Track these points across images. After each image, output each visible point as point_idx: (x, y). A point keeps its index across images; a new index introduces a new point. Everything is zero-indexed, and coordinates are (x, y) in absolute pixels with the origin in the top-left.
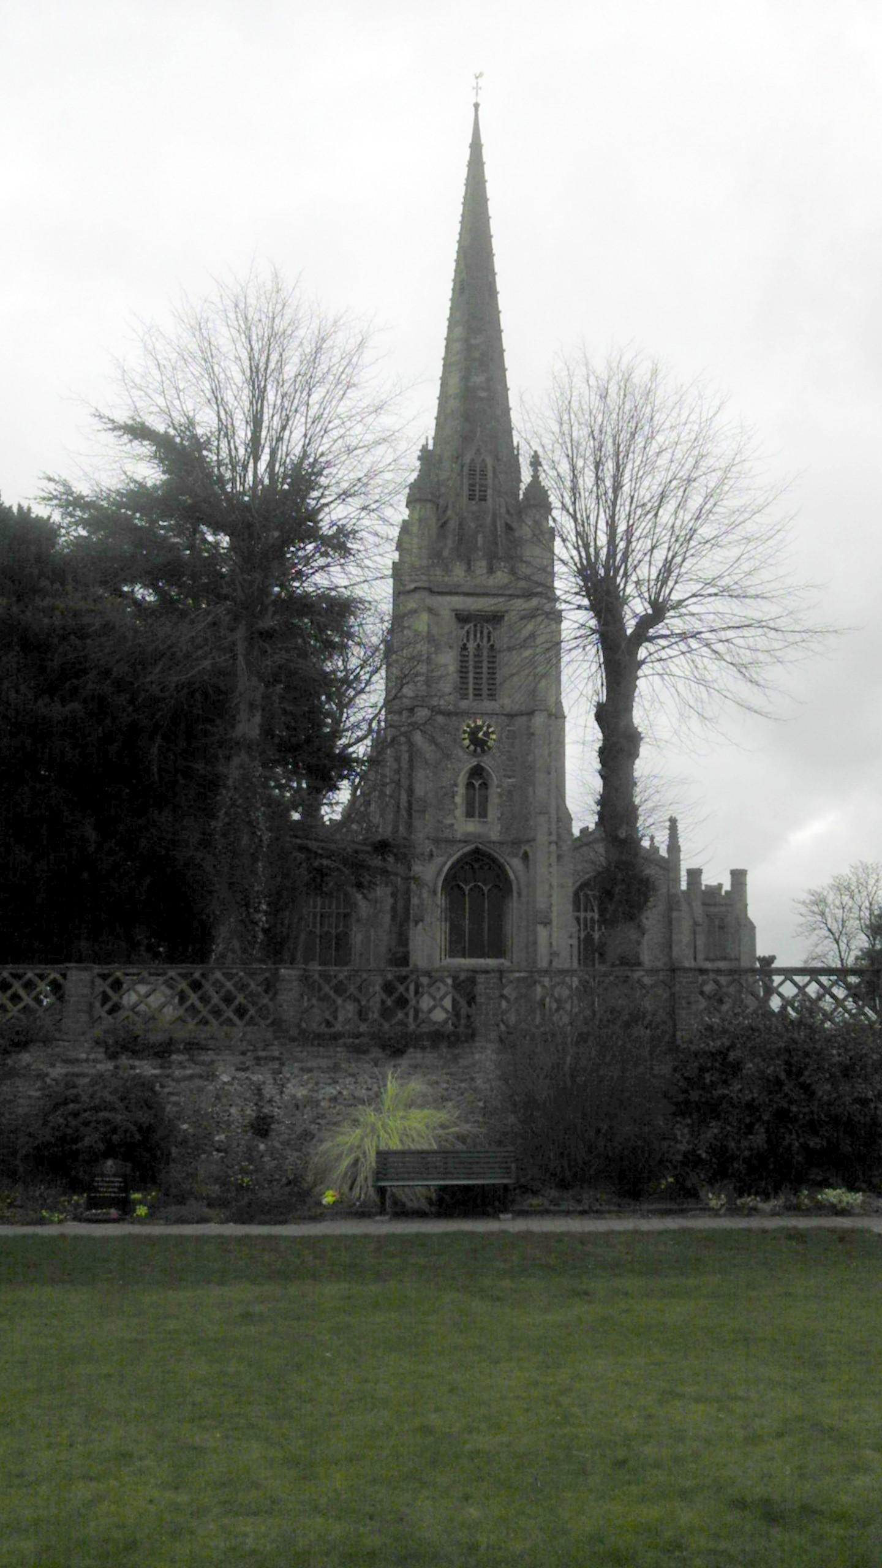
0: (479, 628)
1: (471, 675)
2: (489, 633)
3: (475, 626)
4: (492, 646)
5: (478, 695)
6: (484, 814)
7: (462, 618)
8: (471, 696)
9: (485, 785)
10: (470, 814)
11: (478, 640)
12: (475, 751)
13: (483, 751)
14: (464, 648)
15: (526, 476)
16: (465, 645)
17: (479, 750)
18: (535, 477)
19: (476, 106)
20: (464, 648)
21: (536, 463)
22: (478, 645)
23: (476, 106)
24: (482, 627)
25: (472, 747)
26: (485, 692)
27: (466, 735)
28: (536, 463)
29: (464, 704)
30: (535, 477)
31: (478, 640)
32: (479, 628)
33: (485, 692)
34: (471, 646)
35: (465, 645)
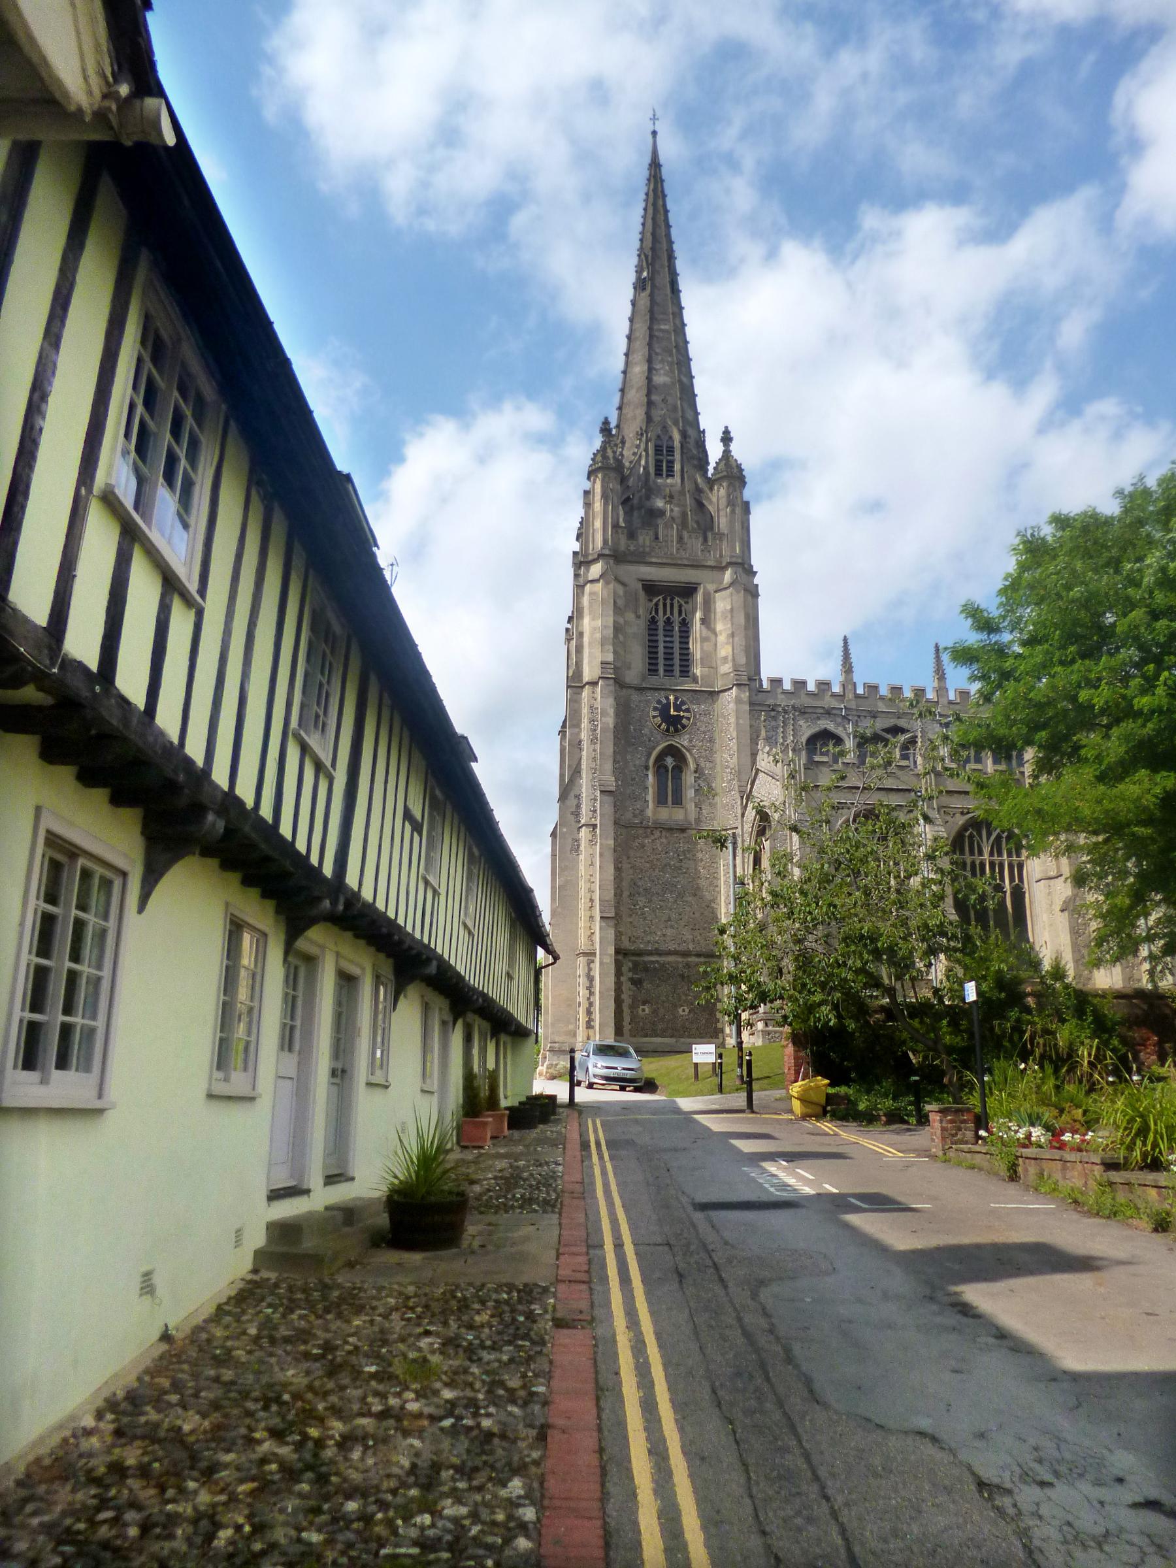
0: (668, 601)
1: (661, 645)
2: (680, 606)
3: (665, 599)
4: (684, 620)
5: (669, 671)
6: (678, 801)
7: (651, 589)
8: (661, 672)
9: (679, 768)
10: (661, 800)
11: (668, 614)
12: (668, 730)
13: (677, 730)
14: (653, 621)
15: (714, 450)
16: (653, 618)
17: (672, 729)
18: (727, 454)
19: (654, 133)
20: (653, 621)
21: (727, 438)
22: (668, 619)
23: (654, 133)
24: (672, 599)
25: (664, 726)
26: (677, 668)
27: (657, 713)
28: (727, 438)
29: (654, 681)
30: (727, 454)
31: (668, 614)
32: (668, 601)
33: (677, 668)
34: (661, 618)
35: (653, 618)
